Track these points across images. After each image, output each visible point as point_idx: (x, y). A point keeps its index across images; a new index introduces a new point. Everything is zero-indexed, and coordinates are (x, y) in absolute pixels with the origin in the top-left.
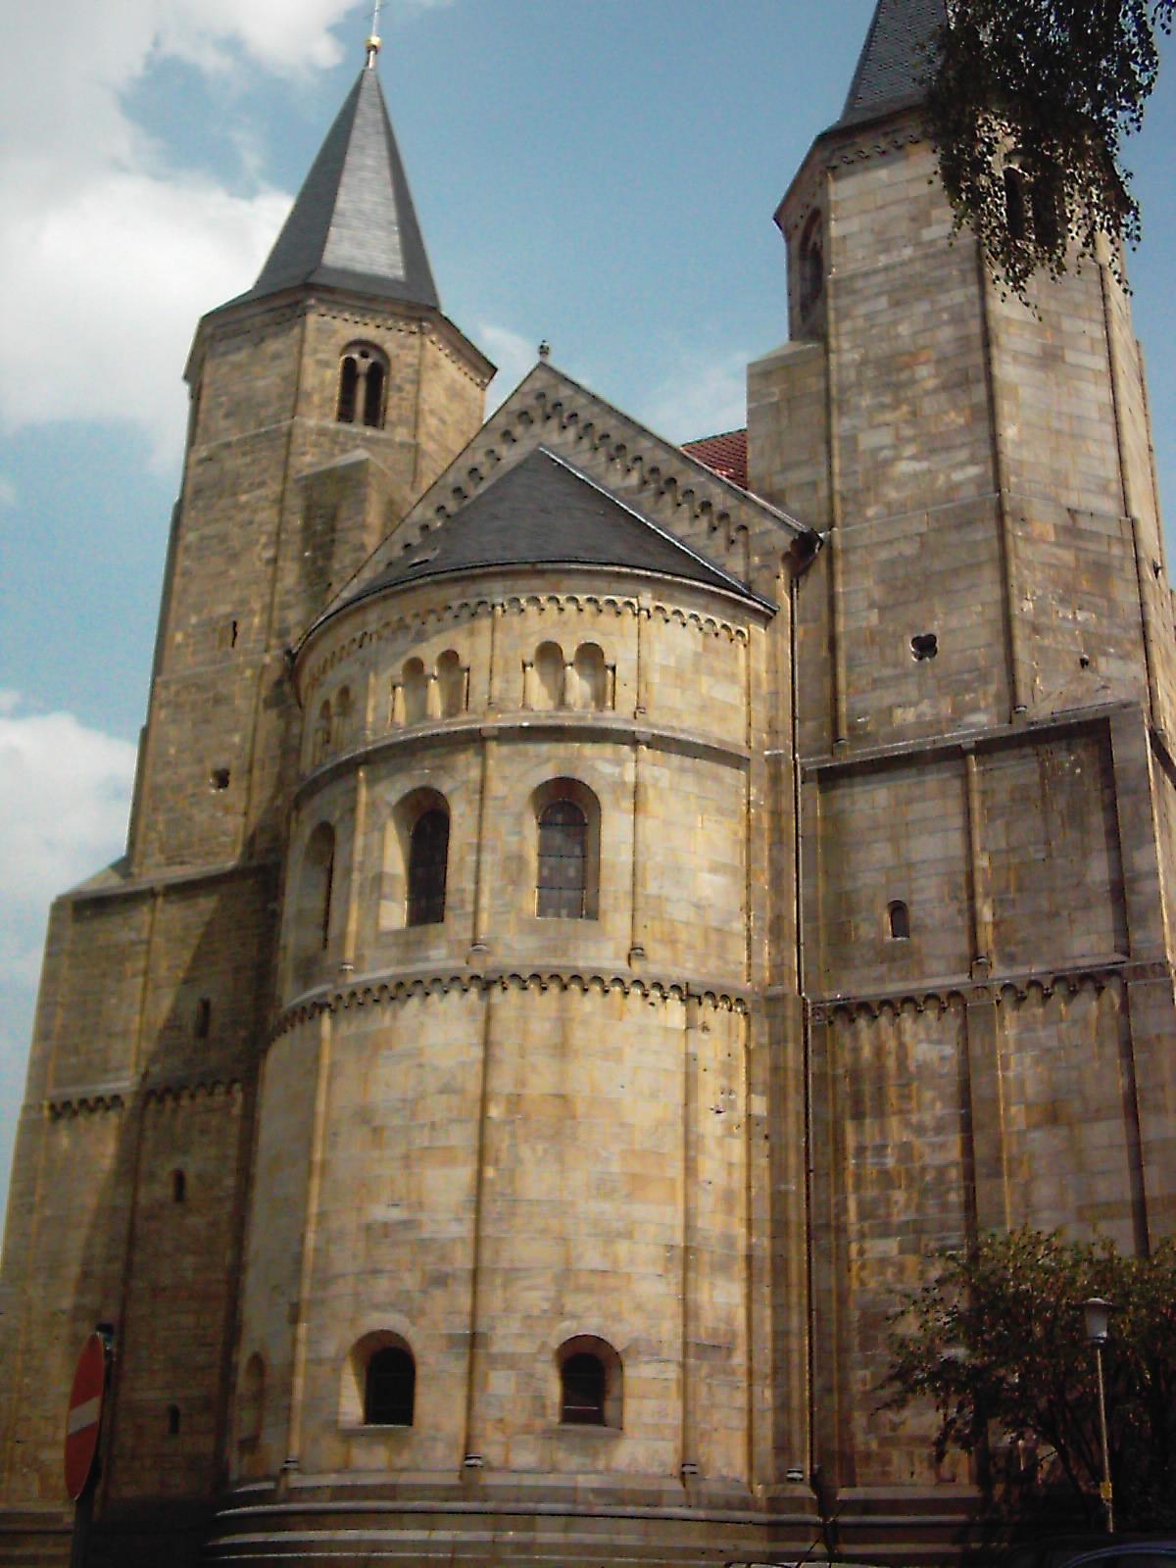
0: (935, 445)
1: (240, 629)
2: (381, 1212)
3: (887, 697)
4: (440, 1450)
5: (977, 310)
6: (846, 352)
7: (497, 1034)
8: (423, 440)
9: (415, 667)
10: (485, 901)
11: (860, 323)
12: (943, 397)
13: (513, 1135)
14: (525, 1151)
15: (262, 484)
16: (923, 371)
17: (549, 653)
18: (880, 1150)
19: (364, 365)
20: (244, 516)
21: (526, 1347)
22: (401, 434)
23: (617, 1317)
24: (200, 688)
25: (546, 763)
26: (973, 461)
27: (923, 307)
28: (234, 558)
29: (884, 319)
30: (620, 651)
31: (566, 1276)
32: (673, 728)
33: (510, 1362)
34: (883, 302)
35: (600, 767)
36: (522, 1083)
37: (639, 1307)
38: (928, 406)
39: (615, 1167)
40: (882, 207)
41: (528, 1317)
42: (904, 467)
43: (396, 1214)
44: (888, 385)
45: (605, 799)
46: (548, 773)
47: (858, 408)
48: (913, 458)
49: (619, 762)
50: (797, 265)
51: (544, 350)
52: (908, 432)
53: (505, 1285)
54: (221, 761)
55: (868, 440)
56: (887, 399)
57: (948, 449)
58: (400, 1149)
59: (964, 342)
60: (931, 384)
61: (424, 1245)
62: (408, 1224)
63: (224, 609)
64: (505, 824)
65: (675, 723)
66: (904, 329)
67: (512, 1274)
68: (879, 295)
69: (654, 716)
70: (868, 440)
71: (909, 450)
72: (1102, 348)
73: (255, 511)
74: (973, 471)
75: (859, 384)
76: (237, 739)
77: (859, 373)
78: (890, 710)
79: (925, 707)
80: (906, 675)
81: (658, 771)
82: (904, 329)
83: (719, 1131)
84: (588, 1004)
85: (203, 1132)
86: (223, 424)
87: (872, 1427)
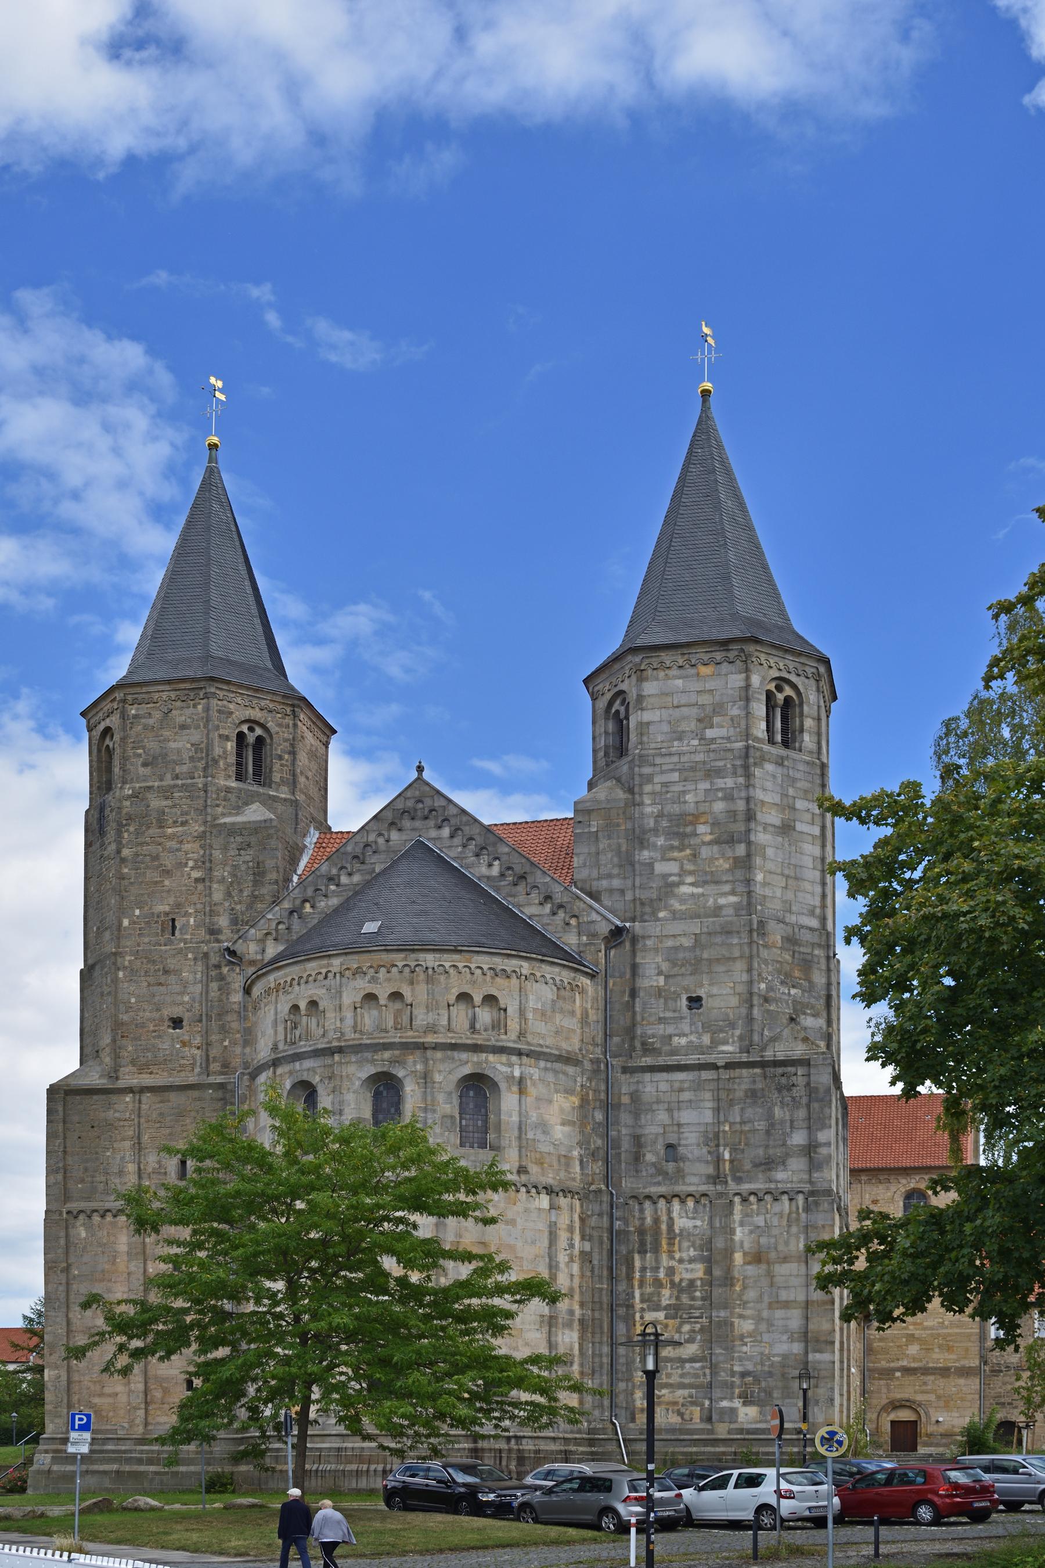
1: (178, 924)
12: (715, 848)
28: (167, 873)
42: (685, 889)
47: (655, 846)
48: (692, 884)
52: (689, 867)
54: (176, 1012)
56: (676, 843)
60: (708, 838)
71: (690, 879)
86: (142, 770)
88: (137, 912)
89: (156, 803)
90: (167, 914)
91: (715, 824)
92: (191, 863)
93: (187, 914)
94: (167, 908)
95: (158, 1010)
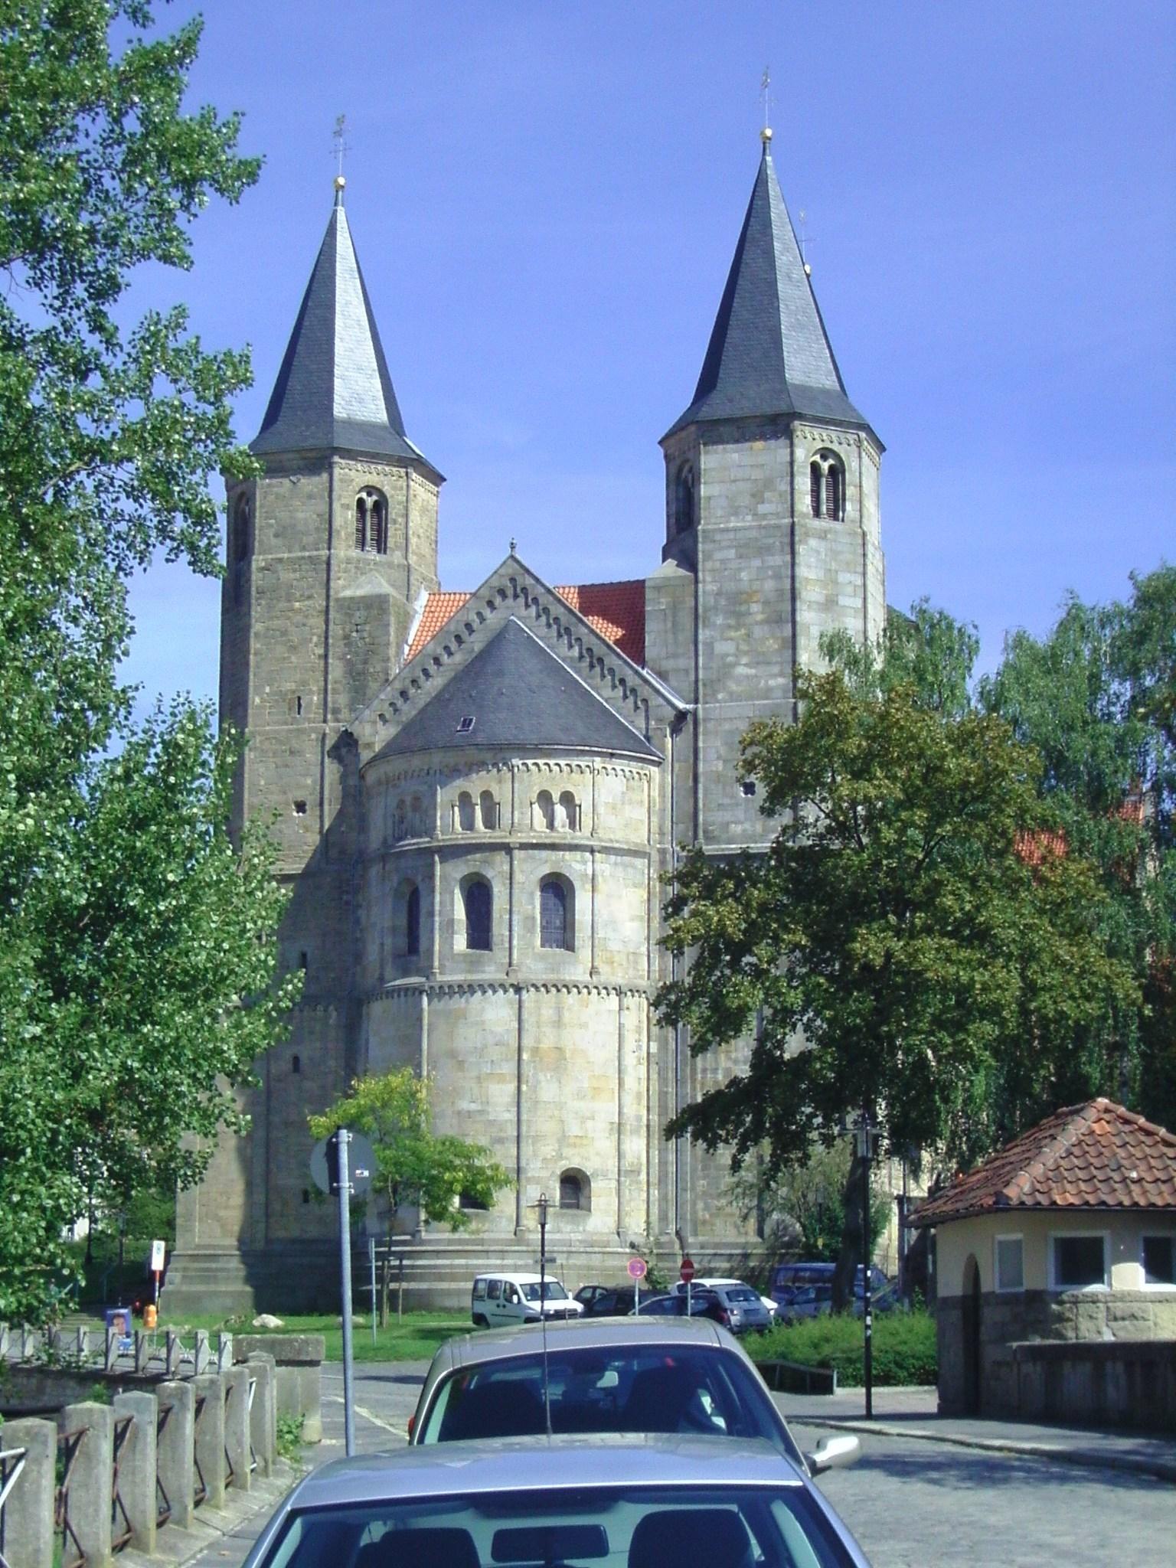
0: (760, 660)
2: (465, 1105)
3: (727, 816)
4: (504, 1222)
5: (789, 573)
6: (708, 585)
7: (525, 1016)
8: (413, 559)
9: (465, 799)
10: (515, 942)
11: (717, 564)
12: (766, 628)
13: (535, 1068)
14: (541, 1077)
15: (310, 597)
16: (755, 608)
17: (545, 797)
18: (715, 1070)
19: (370, 502)
20: (299, 618)
21: (544, 1174)
22: (396, 557)
23: (587, 1159)
24: (281, 743)
25: (545, 864)
26: (781, 674)
27: (756, 563)
28: (293, 649)
29: (733, 565)
30: (583, 798)
31: (563, 1139)
32: (611, 841)
33: (537, 1181)
34: (732, 553)
35: (574, 866)
36: (538, 1041)
37: (598, 1154)
38: (758, 632)
39: (586, 1085)
40: (734, 481)
41: (545, 1159)
42: (741, 670)
43: (473, 1107)
44: (734, 612)
45: (577, 885)
46: (546, 870)
47: (715, 625)
48: (745, 665)
49: (585, 863)
50: (673, 487)
51: (513, 546)
52: (744, 647)
53: (533, 1144)
54: (300, 796)
55: (721, 647)
56: (732, 622)
57: (769, 663)
58: (474, 1074)
59: (780, 592)
60: (760, 617)
61: (492, 1123)
62: (481, 1112)
63: (290, 686)
64: (524, 899)
65: (612, 837)
66: (744, 575)
67: (536, 1139)
68: (729, 547)
69: (601, 833)
70: (721, 647)
71: (744, 660)
72: (860, 592)
73: (306, 617)
74: (781, 681)
75: (715, 608)
76: (309, 781)
77: (716, 601)
78: (728, 824)
79: (747, 826)
80: (737, 805)
81: (604, 865)
82: (744, 575)
83: (635, 1062)
84: (571, 999)
85: (311, 1033)
86: (274, 541)
87: (707, 1208)
88: (267, 690)
89: (286, 576)
90: (294, 692)
91: (766, 603)
92: (315, 639)
93: (311, 692)
94: (293, 686)
95: (285, 793)
